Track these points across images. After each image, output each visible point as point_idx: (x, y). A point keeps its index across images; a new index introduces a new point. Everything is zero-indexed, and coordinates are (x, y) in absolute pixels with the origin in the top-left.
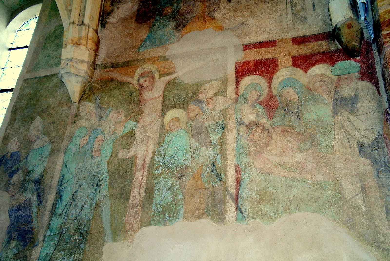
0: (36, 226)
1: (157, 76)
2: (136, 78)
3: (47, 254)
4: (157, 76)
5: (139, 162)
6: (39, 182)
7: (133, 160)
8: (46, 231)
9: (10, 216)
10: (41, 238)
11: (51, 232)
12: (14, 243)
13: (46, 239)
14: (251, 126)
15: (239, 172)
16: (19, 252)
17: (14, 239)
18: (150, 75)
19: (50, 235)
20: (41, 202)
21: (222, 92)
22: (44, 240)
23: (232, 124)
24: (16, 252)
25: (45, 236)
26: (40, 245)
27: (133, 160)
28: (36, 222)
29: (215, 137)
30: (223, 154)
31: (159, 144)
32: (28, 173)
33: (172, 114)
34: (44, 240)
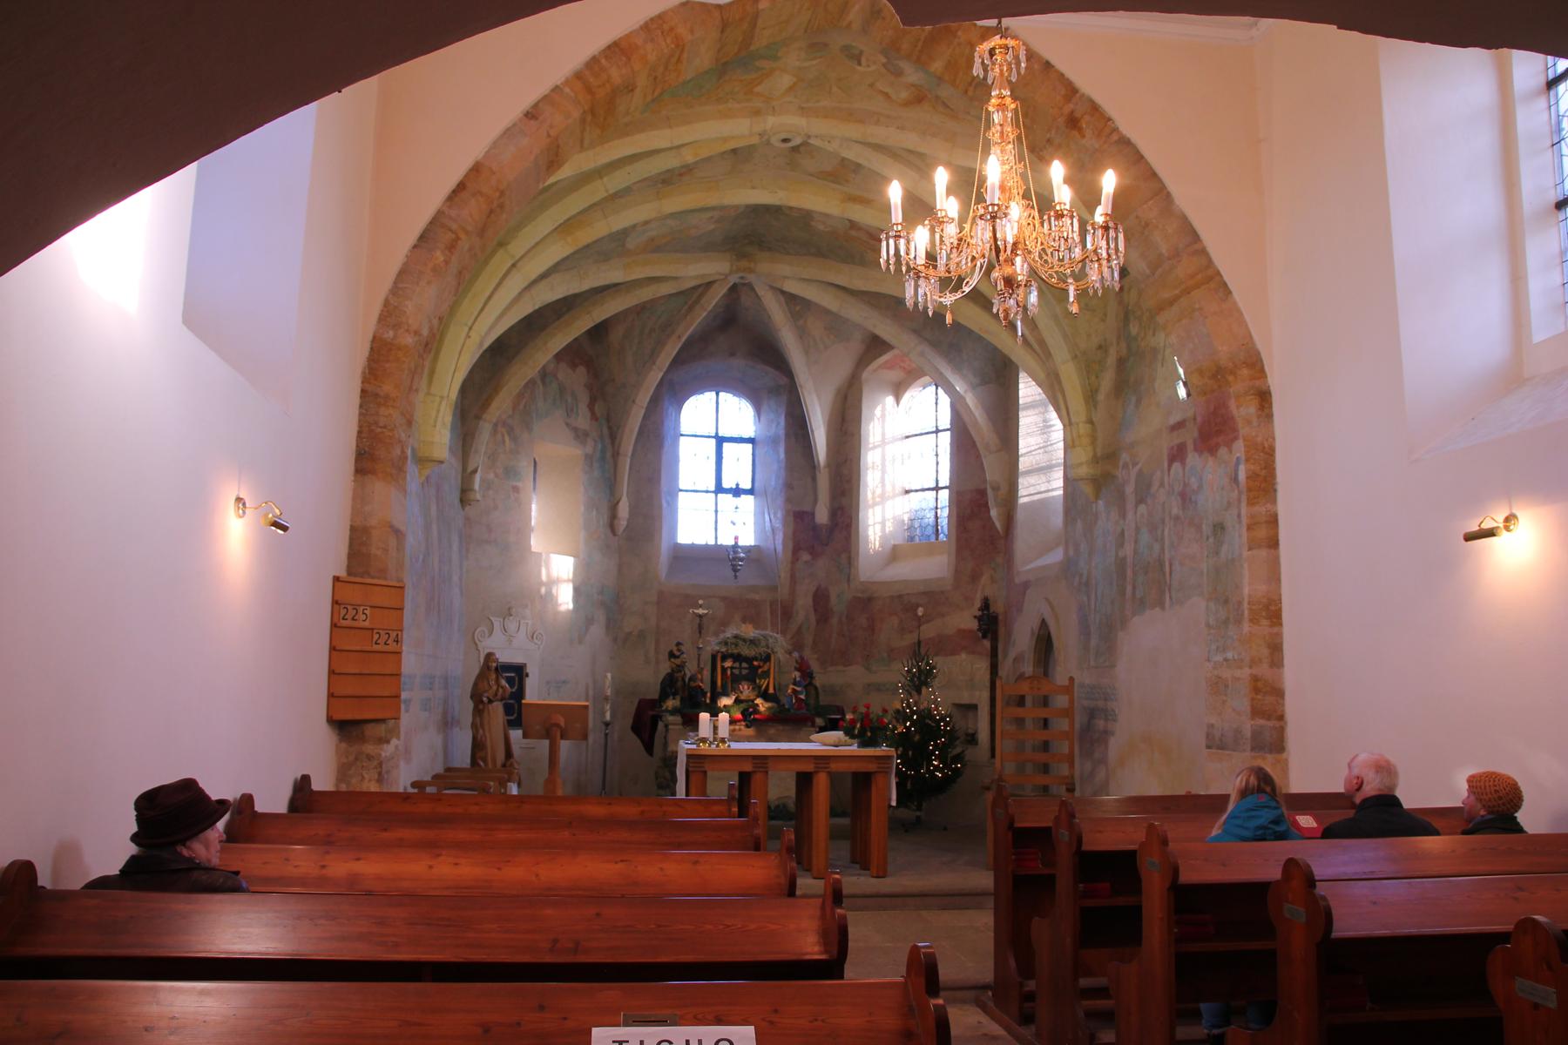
1: (1131, 467)
2: (1120, 470)
4: (1131, 467)
5: (1128, 560)
6: (1087, 584)
7: (1124, 559)
14: (1177, 518)
15: (1171, 565)
18: (1126, 466)
21: (1162, 485)
23: (1167, 519)
27: (1124, 559)
29: (1159, 532)
30: (1163, 549)
31: (1136, 542)
32: (1081, 575)
33: (1142, 508)
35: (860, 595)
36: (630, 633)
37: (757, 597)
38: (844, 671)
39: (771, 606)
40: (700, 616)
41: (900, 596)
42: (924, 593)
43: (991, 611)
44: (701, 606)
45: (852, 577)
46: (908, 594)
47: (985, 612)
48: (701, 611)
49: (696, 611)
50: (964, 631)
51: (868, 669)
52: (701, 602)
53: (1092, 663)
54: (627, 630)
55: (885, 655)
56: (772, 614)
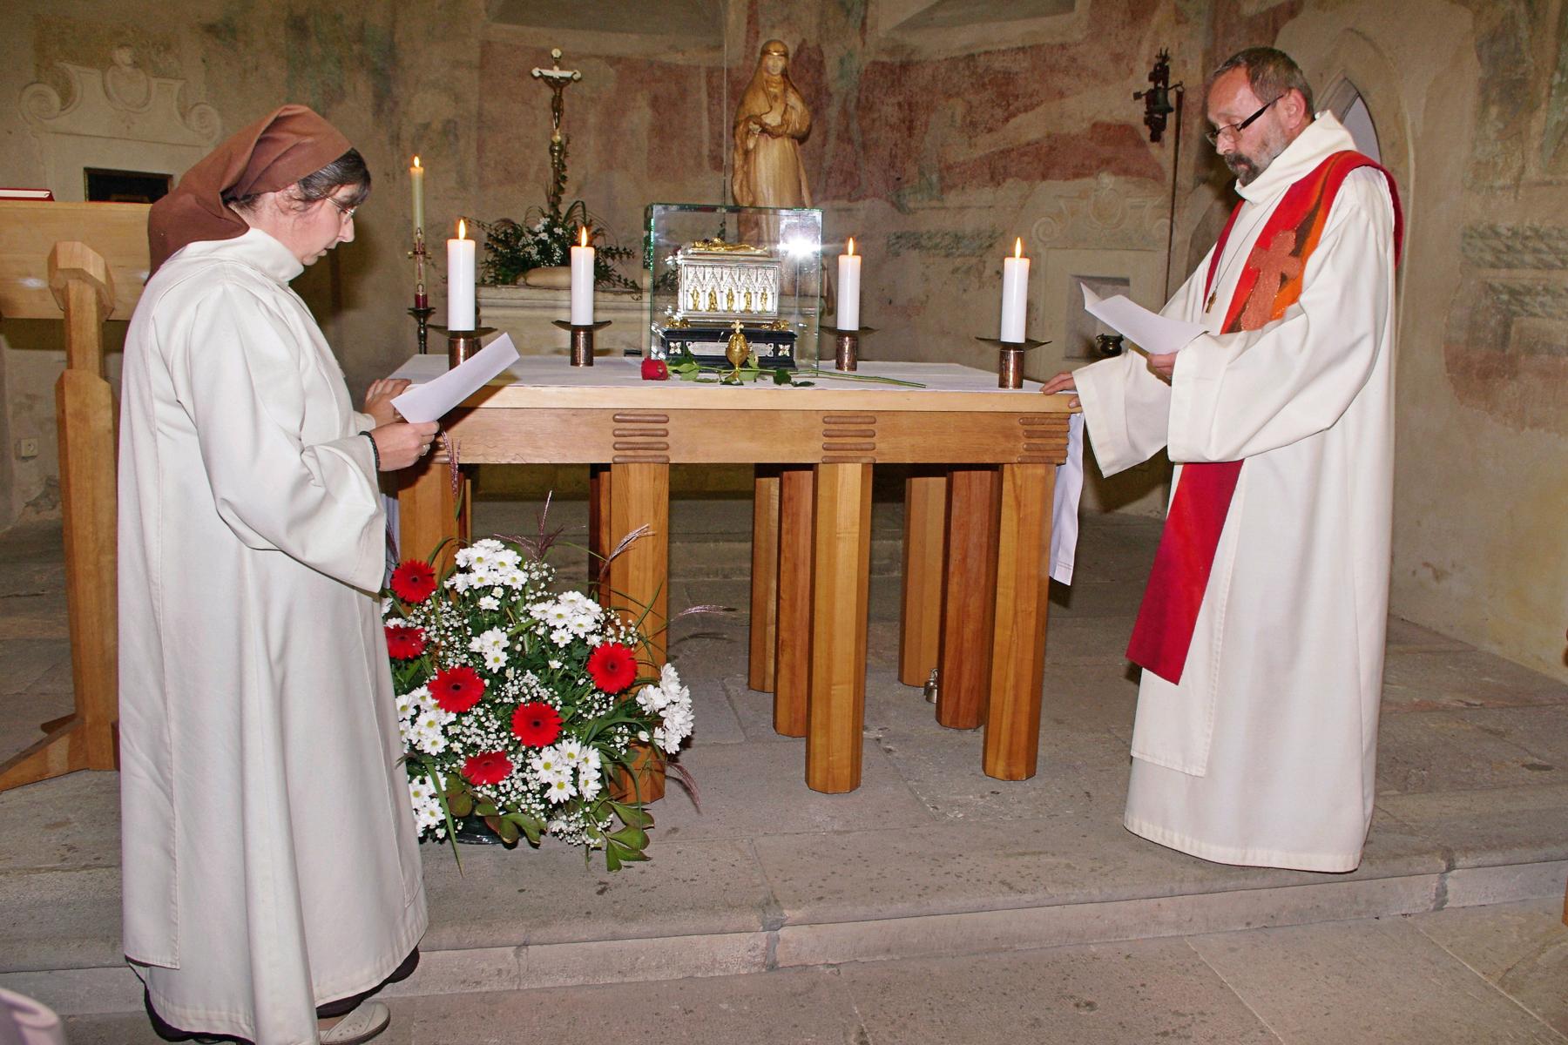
0: (1533, 68)
3: (1558, 122)
8: (1552, 76)
9: (1479, 57)
10: (1544, 93)
11: (1562, 77)
12: (1494, 111)
13: (1554, 92)
16: (1506, 127)
17: (1493, 102)
19: (1560, 83)
20: (1535, 14)
22: (1549, 95)
24: (1501, 126)
25: (1551, 87)
26: (1543, 106)
28: (1532, 60)
34: (1549, 95)
35: (884, 58)
36: (427, 126)
37: (679, 59)
38: (849, 210)
39: (710, 73)
40: (556, 84)
41: (971, 57)
42: (1022, 49)
43: (1172, 81)
44: (556, 62)
45: (869, 21)
46: (986, 53)
47: (1160, 85)
48: (556, 73)
49: (547, 72)
50: (1108, 127)
51: (899, 206)
52: (556, 53)
53: (1532, 173)
54: (419, 120)
55: (935, 178)
56: (709, 95)
